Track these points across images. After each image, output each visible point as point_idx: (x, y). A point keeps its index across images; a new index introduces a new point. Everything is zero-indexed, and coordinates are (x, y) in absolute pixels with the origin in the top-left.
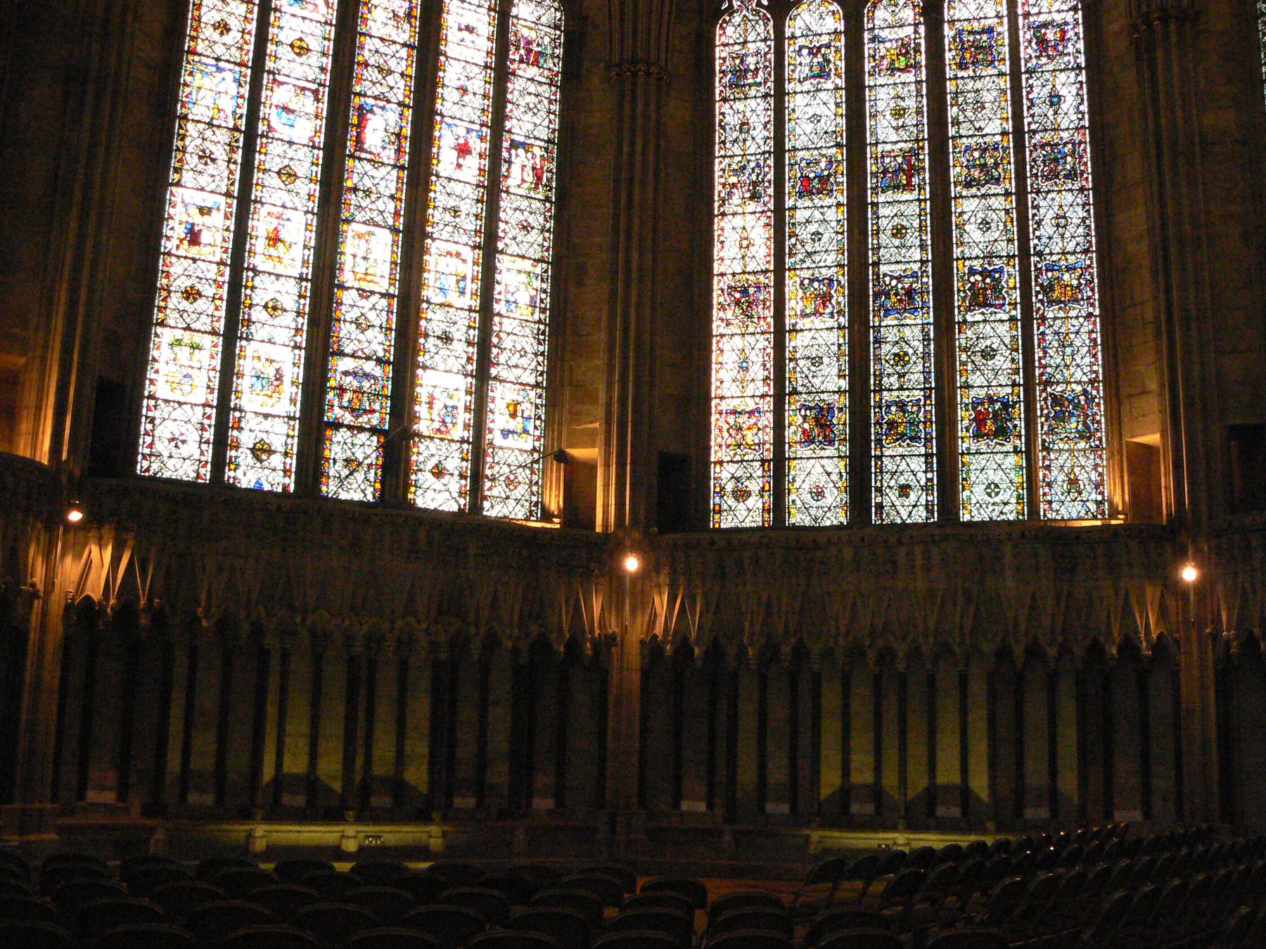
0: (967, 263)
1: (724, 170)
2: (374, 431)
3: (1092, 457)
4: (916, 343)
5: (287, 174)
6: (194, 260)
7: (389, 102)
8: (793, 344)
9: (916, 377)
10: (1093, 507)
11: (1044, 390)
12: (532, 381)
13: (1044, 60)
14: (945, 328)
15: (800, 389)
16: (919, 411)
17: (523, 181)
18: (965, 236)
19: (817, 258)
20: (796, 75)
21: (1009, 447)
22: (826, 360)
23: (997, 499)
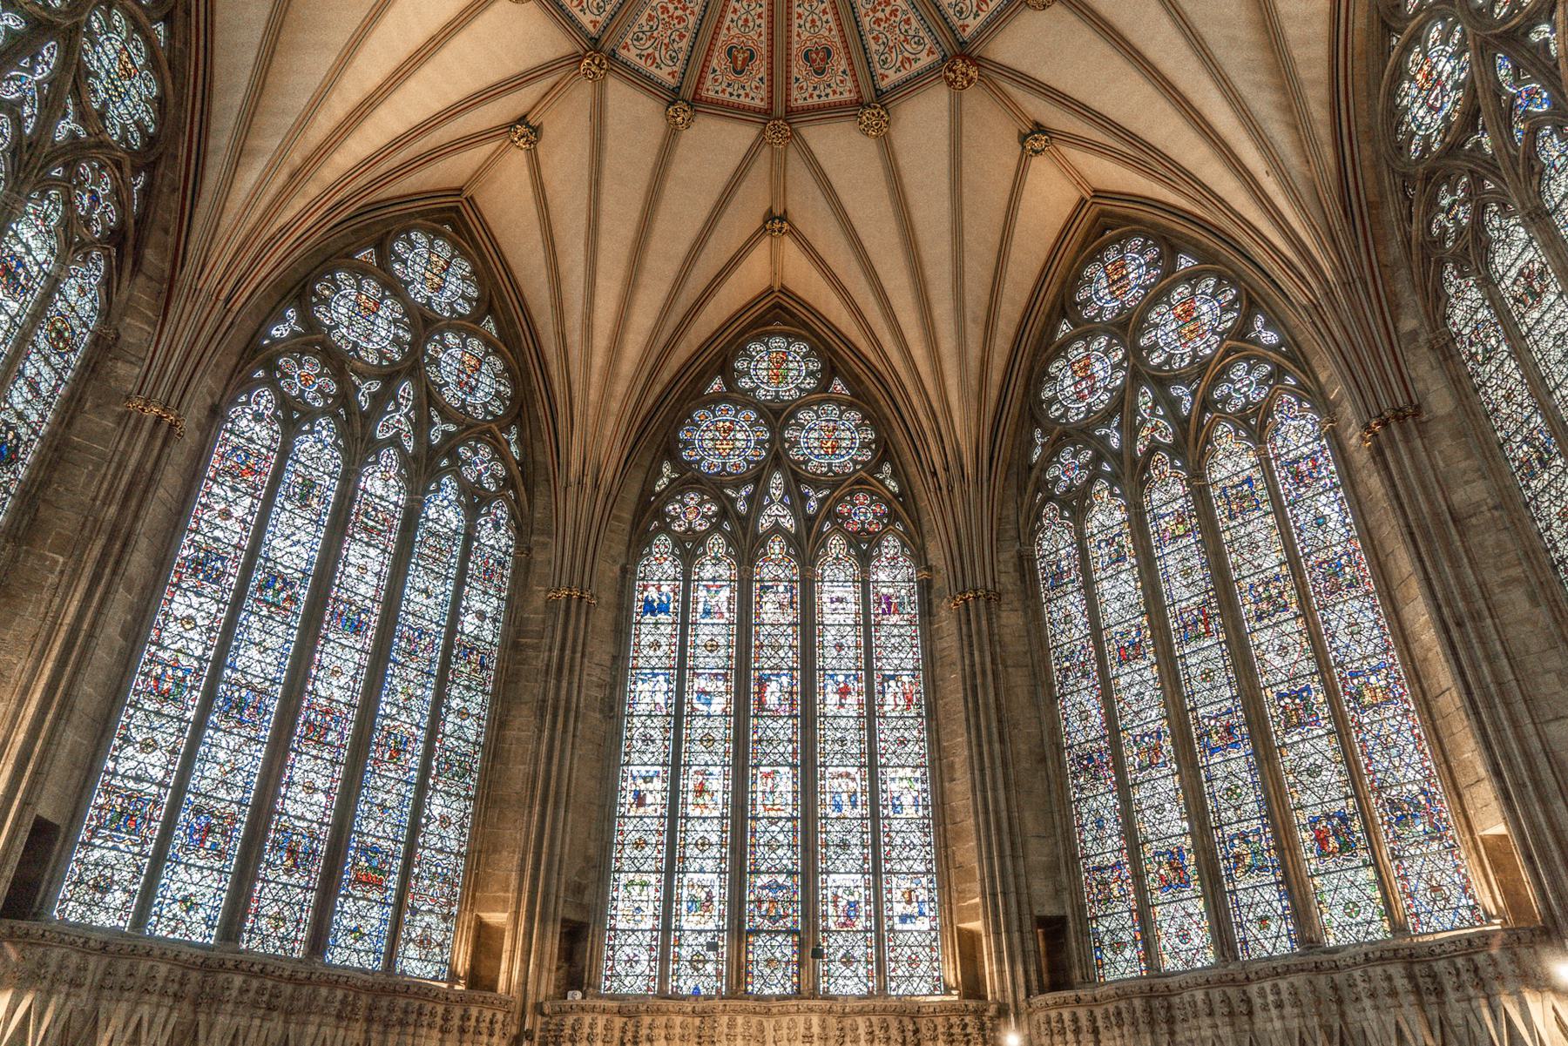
0: (1274, 689)
1: (1058, 658)
2: (789, 932)
3: (1450, 858)
4: (1245, 774)
5: (708, 740)
6: (641, 818)
7: (781, 669)
8: (1137, 796)
9: (1251, 806)
10: (1466, 913)
11: (1379, 797)
12: (922, 868)
13: (1303, 490)
14: (1265, 756)
15: (1151, 837)
16: (1261, 840)
17: (897, 705)
18: (1267, 665)
19: (1143, 715)
20: (1100, 566)
21: (1357, 862)
22: (1167, 806)
23: (1359, 919)
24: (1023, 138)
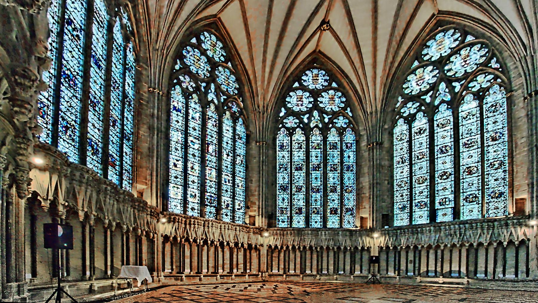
14: (325, 195)
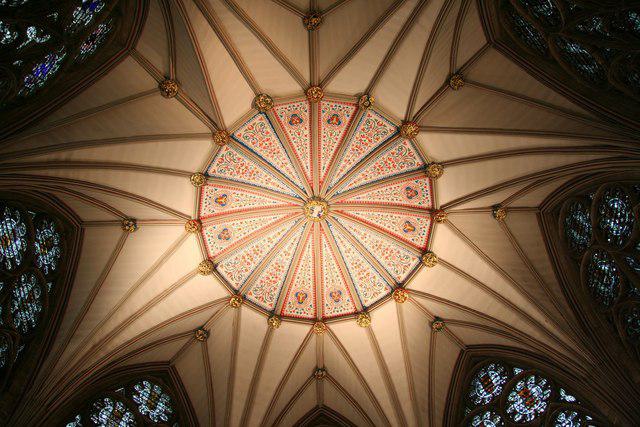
24: (431, 324)
